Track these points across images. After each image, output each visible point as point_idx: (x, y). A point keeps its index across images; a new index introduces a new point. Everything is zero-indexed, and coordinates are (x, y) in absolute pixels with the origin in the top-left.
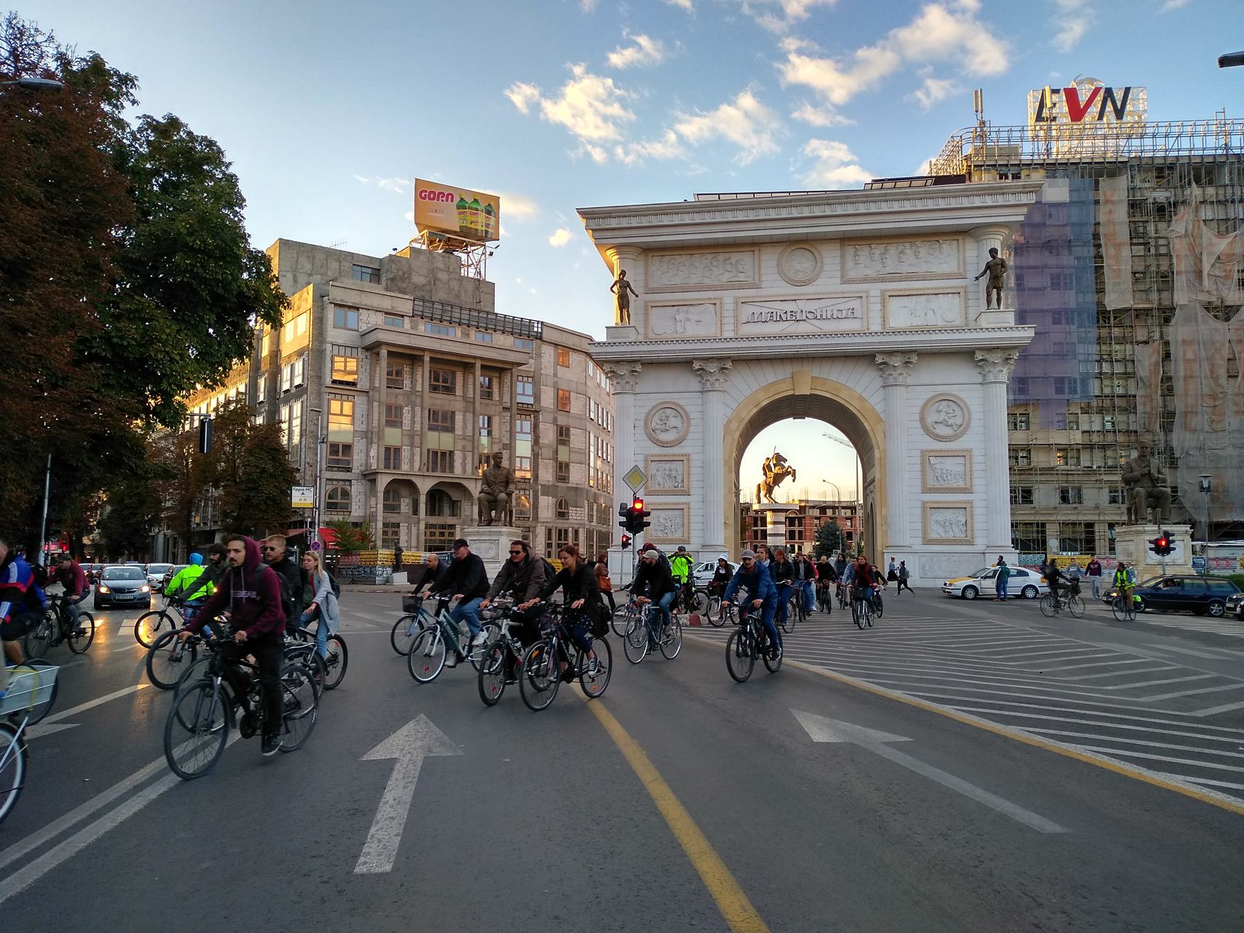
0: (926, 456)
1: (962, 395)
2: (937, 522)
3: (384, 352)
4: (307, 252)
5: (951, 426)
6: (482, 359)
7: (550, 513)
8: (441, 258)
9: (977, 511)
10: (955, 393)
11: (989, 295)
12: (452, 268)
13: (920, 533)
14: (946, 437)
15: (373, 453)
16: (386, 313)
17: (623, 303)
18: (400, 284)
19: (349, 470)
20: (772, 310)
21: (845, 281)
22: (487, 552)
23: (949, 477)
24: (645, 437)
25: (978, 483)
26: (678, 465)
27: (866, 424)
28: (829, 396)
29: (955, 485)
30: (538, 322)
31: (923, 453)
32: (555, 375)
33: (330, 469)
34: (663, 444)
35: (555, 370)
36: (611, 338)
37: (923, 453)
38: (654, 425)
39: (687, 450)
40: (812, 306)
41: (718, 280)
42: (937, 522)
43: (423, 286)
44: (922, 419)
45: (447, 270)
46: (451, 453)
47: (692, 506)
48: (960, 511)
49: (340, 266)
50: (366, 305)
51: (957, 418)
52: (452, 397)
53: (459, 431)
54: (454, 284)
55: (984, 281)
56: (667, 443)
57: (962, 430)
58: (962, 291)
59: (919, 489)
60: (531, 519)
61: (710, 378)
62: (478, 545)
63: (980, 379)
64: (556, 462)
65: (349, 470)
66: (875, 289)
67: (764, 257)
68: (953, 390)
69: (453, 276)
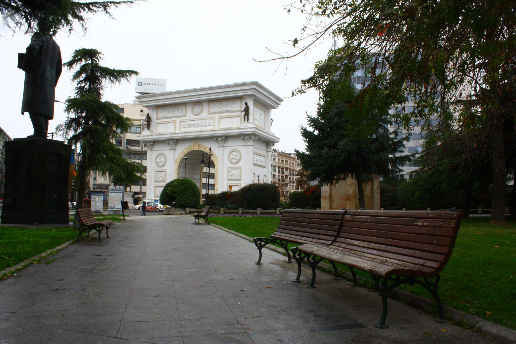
1: (239, 149)
5: (235, 159)
10: (238, 149)
11: (244, 117)
14: (234, 163)
21: (209, 114)
24: (155, 164)
26: (163, 173)
40: (199, 122)
48: (237, 187)
55: (244, 113)
57: (239, 160)
58: (240, 116)
66: (217, 116)
67: (187, 107)
68: (237, 148)
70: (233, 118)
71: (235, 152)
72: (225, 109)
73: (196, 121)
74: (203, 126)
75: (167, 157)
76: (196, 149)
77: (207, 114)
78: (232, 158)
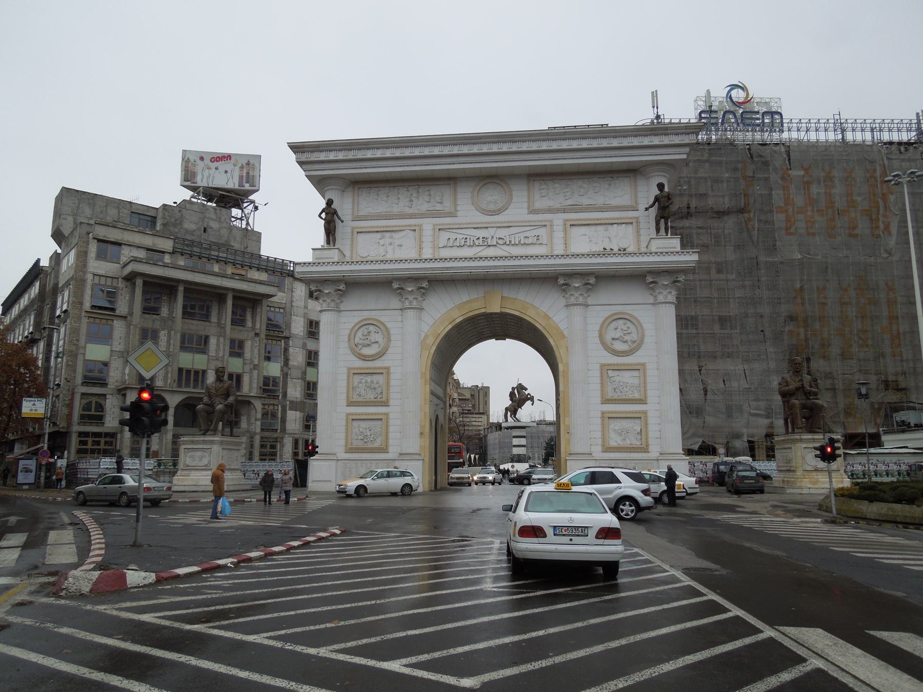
0: (605, 369)
1: (635, 314)
2: (615, 430)
3: (139, 282)
4: (89, 199)
5: (626, 342)
6: (234, 290)
7: (297, 426)
8: (212, 210)
9: (651, 421)
10: (629, 312)
11: (658, 223)
12: (223, 218)
13: (600, 442)
14: (623, 352)
15: (127, 371)
16: (148, 249)
17: (330, 231)
18: (172, 228)
19: (104, 385)
20: (465, 237)
22: (201, 460)
23: (625, 389)
25: (652, 395)
27: (551, 340)
28: (517, 314)
29: (630, 397)
30: (290, 262)
31: (602, 366)
32: (306, 307)
33: (85, 383)
34: (364, 358)
35: (306, 302)
36: (317, 259)
37: (602, 366)
38: (357, 340)
39: (386, 364)
40: (502, 233)
41: (418, 209)
42: (615, 430)
43: (194, 231)
44: (601, 337)
45: (219, 220)
46: (204, 372)
47: (391, 416)
49: (119, 212)
50: (128, 241)
51: (632, 335)
52: (207, 323)
53: (212, 352)
54: (224, 232)
55: (653, 212)
56: (369, 356)
58: (633, 221)
59: (599, 400)
60: (279, 431)
61: (409, 297)
62: (192, 453)
63: (651, 300)
64: (305, 381)
65: (104, 385)
66: (558, 219)
68: (628, 309)
69: (224, 225)
70: (610, 227)
71: (621, 322)
72: (585, 201)
73: (492, 231)
74: (513, 245)
75: (392, 332)
76: (495, 308)
77: (526, 211)
78: (613, 339)
